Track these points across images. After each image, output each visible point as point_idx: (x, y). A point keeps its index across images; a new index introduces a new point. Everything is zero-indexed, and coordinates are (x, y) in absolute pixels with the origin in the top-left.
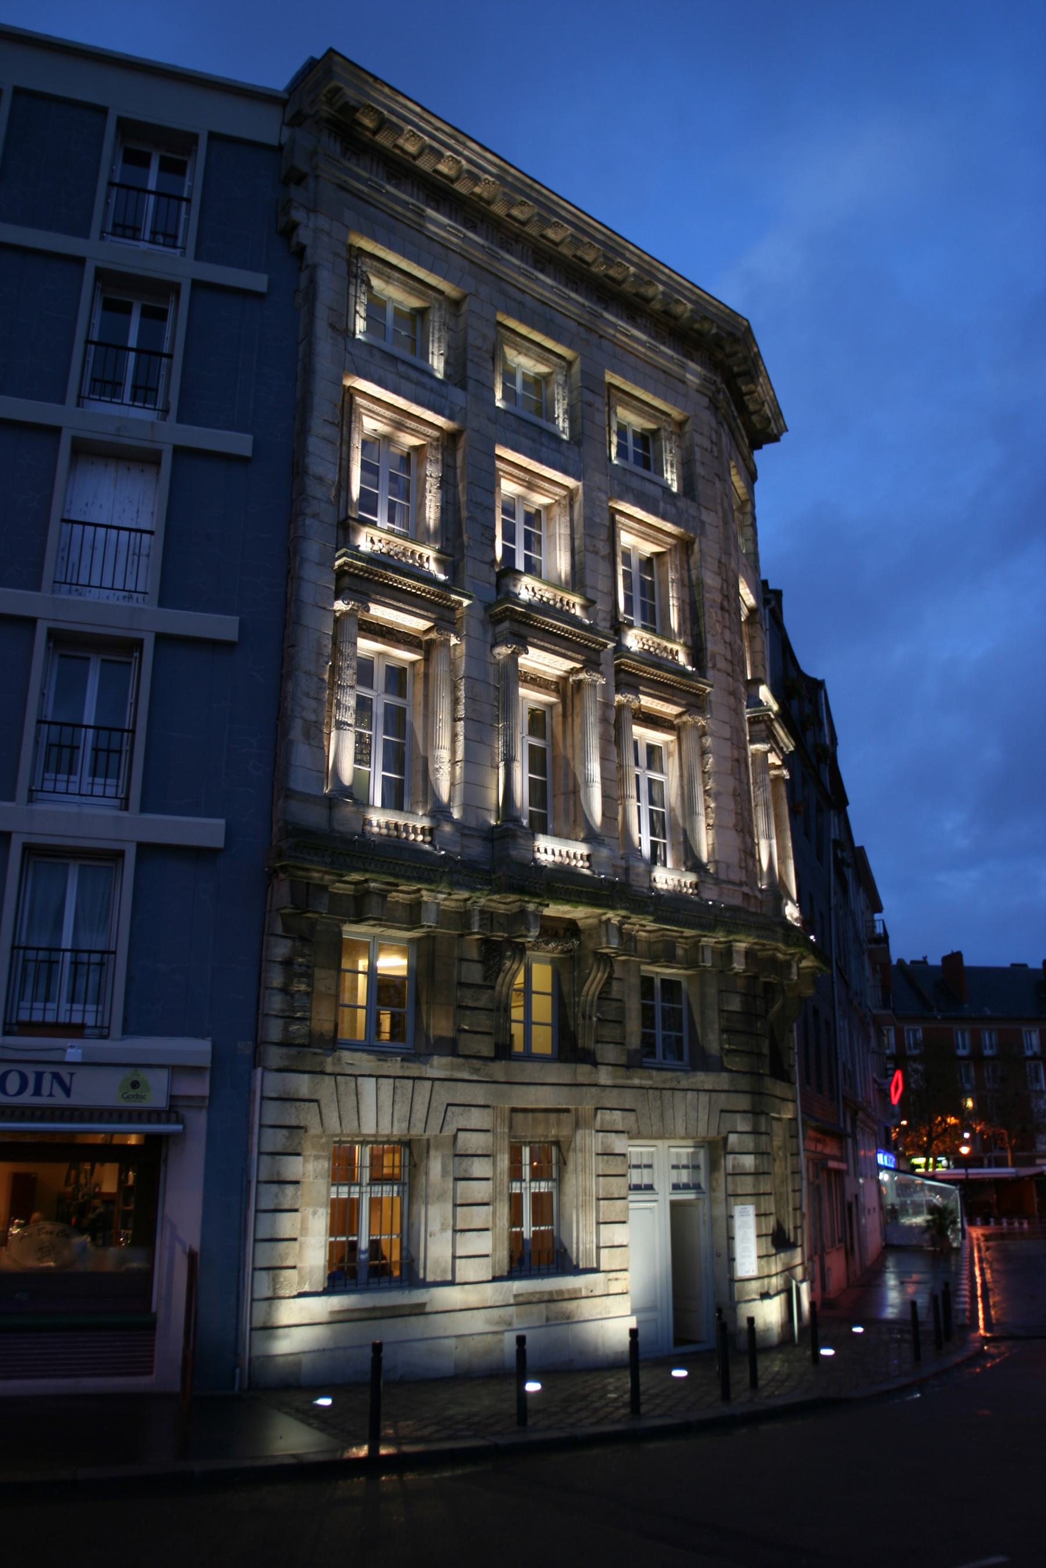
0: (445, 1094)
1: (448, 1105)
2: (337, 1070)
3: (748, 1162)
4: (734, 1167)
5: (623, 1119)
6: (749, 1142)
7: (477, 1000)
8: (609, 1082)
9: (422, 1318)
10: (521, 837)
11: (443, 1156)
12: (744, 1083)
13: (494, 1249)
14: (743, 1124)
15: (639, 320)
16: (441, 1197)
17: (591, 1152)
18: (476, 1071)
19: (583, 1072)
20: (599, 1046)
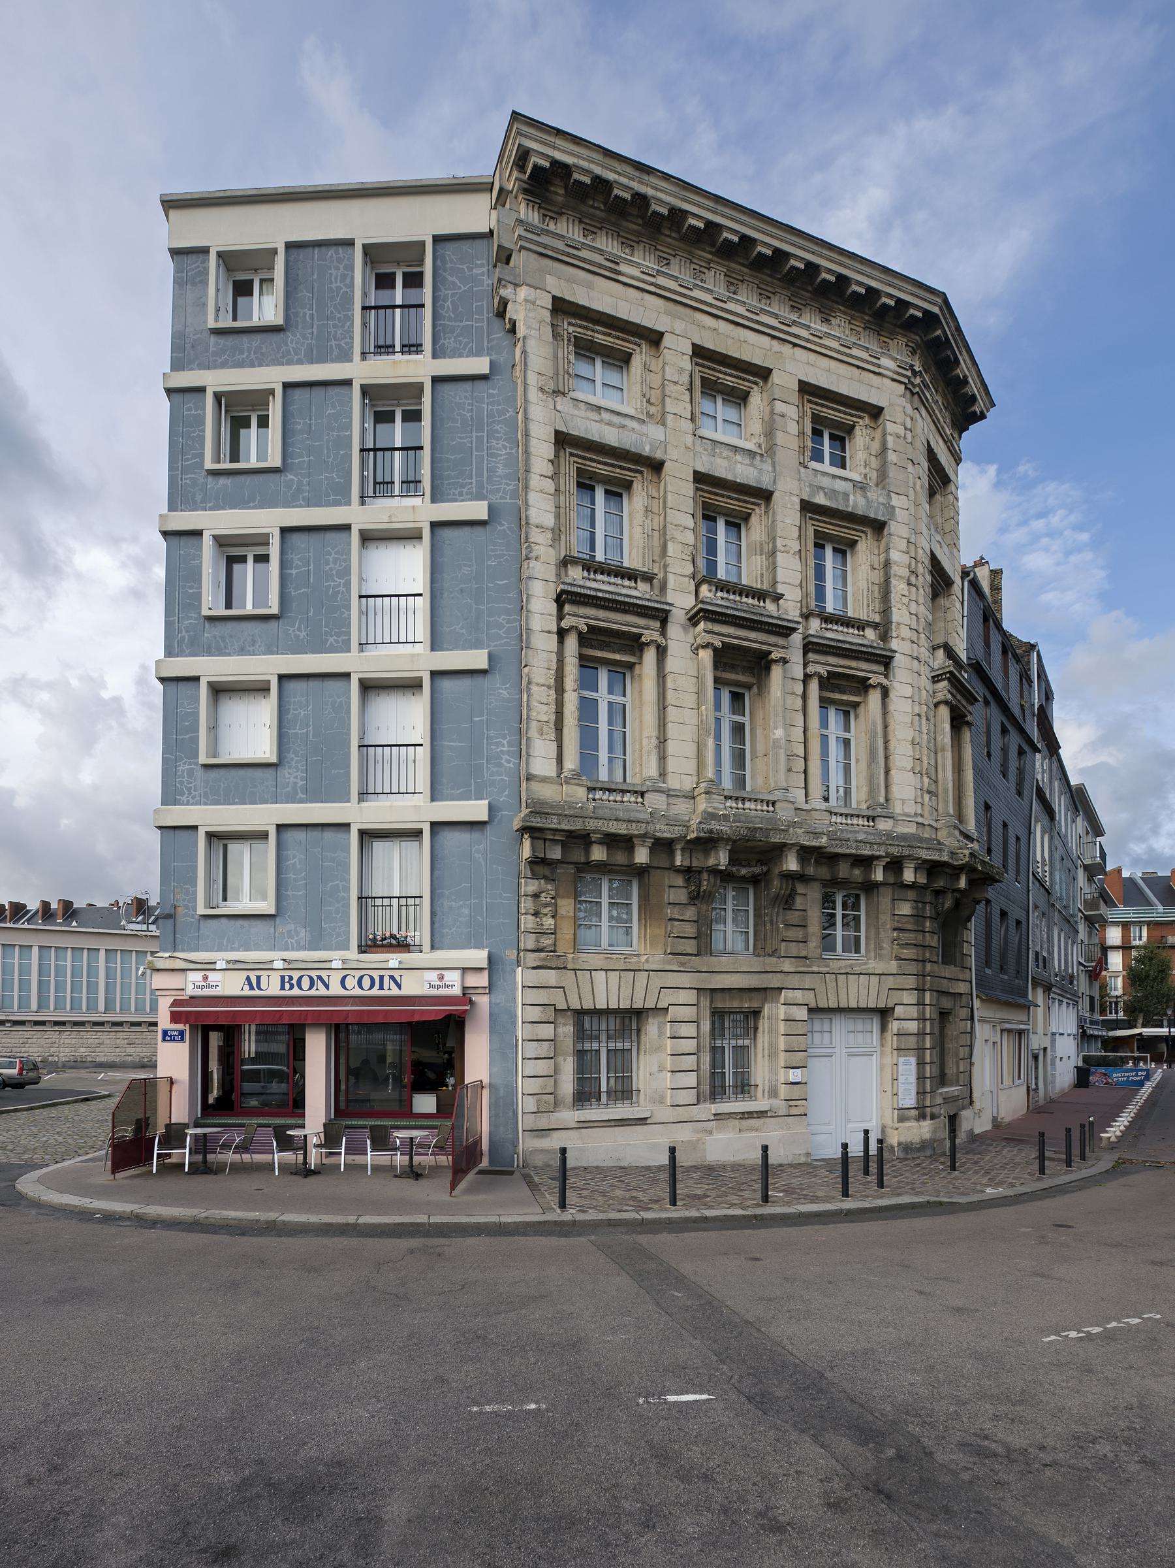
0: (657, 981)
3: (913, 1026)
4: (898, 1030)
5: (803, 996)
6: (914, 1012)
7: (682, 915)
9: (645, 1127)
10: (714, 794)
12: (912, 968)
13: (699, 1084)
14: (910, 998)
15: (833, 321)
16: (658, 1049)
17: (777, 1019)
18: (683, 964)
19: (771, 963)
20: (783, 944)
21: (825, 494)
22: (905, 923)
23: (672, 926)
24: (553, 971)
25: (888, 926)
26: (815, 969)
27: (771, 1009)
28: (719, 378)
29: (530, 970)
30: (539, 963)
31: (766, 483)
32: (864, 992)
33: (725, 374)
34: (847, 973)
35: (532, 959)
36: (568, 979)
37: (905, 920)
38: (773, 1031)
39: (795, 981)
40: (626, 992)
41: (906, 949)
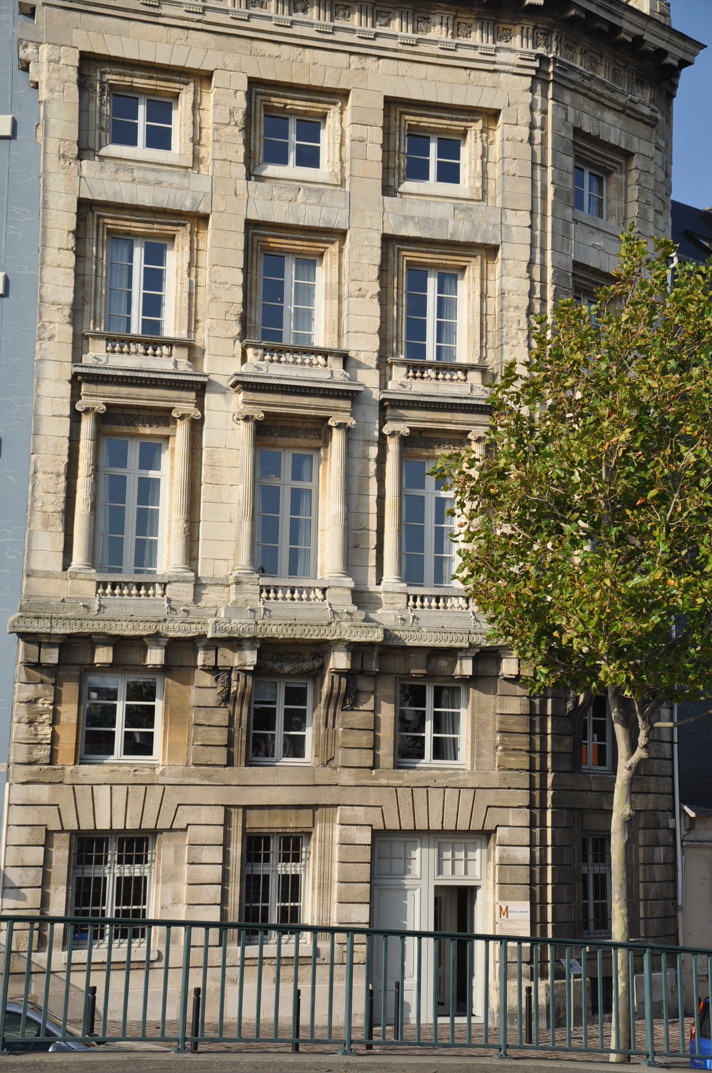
0: (174, 797)
1: (179, 805)
2: (75, 781)
5: (366, 814)
8: (352, 783)
11: (176, 847)
17: (331, 842)
21: (415, 224)
22: (513, 724)
23: (196, 733)
24: (47, 787)
25: (490, 728)
26: (383, 781)
27: (324, 830)
28: (286, 105)
29: (19, 785)
30: (30, 778)
31: (337, 221)
32: (451, 810)
33: (295, 99)
34: (428, 787)
35: (22, 773)
36: (64, 795)
37: (512, 720)
38: (325, 857)
39: (355, 796)
40: (135, 810)
41: (514, 756)
